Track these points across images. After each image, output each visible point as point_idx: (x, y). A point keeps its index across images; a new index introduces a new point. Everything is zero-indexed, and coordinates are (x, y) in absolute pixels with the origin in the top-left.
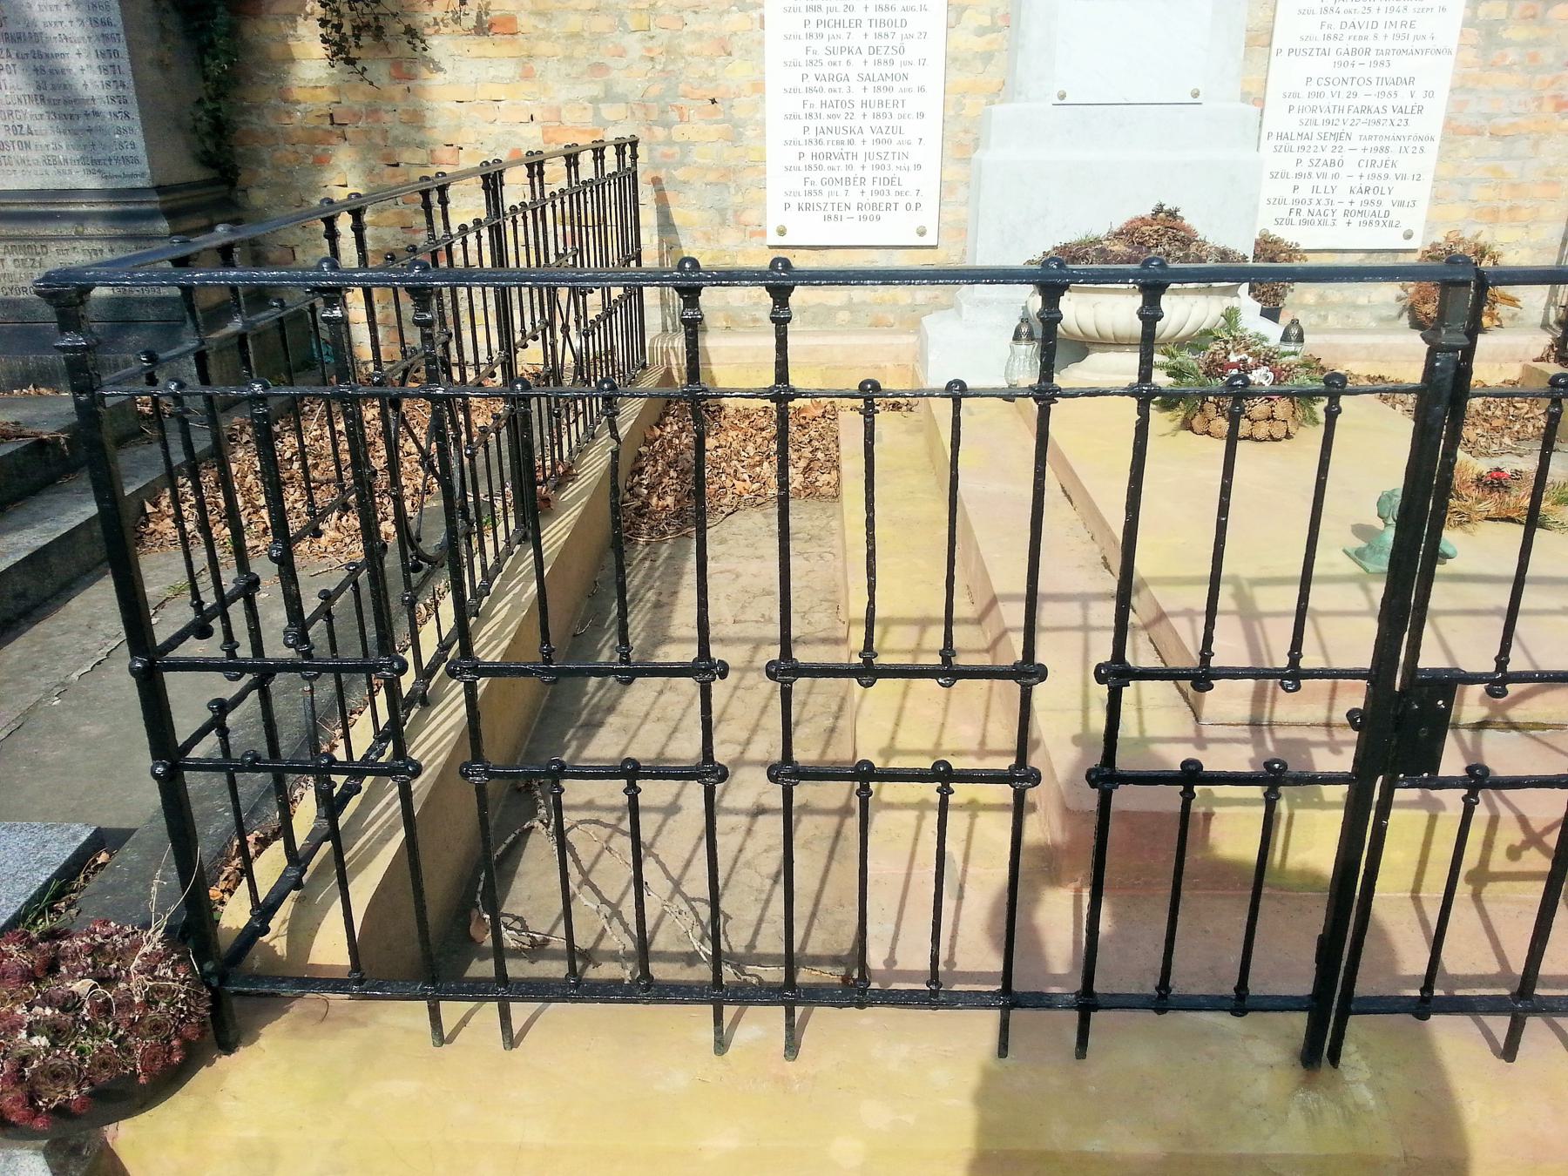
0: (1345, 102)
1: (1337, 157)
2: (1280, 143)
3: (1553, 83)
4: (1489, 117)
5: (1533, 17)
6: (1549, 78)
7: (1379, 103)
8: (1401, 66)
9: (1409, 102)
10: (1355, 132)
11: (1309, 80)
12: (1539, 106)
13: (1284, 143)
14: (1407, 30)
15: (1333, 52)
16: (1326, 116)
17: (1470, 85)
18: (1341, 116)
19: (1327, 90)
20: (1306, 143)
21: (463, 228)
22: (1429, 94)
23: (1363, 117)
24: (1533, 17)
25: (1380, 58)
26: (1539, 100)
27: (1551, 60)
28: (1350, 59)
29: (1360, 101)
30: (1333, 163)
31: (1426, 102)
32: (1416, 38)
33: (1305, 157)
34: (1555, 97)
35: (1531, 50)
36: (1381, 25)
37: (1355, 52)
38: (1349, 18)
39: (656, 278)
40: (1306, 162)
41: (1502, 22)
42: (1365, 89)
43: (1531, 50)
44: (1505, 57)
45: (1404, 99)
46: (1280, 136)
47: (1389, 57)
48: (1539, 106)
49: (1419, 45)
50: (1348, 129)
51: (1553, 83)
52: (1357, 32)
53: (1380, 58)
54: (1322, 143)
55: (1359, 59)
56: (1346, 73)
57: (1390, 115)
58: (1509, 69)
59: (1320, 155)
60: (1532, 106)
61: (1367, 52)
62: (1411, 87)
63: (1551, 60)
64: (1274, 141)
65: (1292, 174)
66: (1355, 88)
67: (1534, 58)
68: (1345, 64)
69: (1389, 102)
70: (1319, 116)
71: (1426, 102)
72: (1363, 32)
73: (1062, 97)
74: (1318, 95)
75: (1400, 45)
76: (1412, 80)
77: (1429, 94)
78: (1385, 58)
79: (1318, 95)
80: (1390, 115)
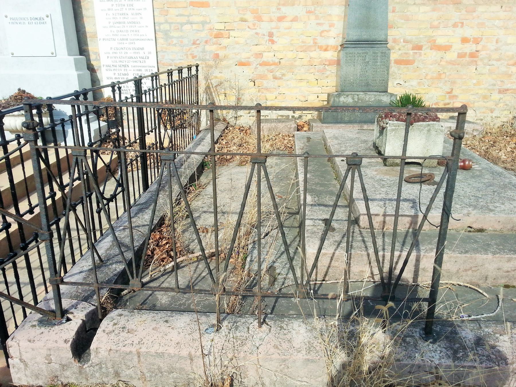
0: (125, 56)
1: (126, 72)
2: (107, 68)
3: (189, 50)
4: (173, 60)
5: (178, 29)
7: (136, 55)
8: (138, 44)
9: (144, 56)
10: (130, 64)
11: (111, 48)
12: (187, 57)
13: (109, 68)
14: (138, 33)
15: (116, 40)
16: (120, 60)
17: (164, 50)
18: (124, 60)
19: (118, 51)
20: (115, 68)
22: (150, 53)
23: (131, 60)
24: (178, 29)
25: (131, 42)
28: (122, 42)
29: (129, 55)
30: (125, 75)
31: (149, 55)
32: (141, 35)
33: (117, 72)
35: (180, 39)
36: (129, 31)
37: (123, 39)
38: (119, 29)
39: (204, 107)
40: (117, 74)
41: (169, 31)
42: (129, 51)
43: (180, 39)
44: (172, 41)
45: (142, 54)
46: (107, 66)
47: (134, 41)
48: (187, 57)
49: (142, 38)
50: (127, 64)
51: (189, 50)
52: (122, 33)
53: (131, 42)
54: (120, 68)
55: (125, 42)
56: (123, 46)
57: (139, 59)
58: (175, 45)
59: (120, 72)
60: (185, 57)
61: (127, 40)
62: (143, 51)
64: (105, 68)
65: (114, 78)
66: (126, 51)
67: (182, 42)
68: (121, 43)
69: (138, 55)
70: (118, 60)
71: (149, 55)
72: (124, 33)
73: (13, 54)
74: (116, 53)
75: (137, 37)
76: (143, 49)
77: (150, 53)
78: (133, 41)
79: (116, 53)
80: (139, 59)
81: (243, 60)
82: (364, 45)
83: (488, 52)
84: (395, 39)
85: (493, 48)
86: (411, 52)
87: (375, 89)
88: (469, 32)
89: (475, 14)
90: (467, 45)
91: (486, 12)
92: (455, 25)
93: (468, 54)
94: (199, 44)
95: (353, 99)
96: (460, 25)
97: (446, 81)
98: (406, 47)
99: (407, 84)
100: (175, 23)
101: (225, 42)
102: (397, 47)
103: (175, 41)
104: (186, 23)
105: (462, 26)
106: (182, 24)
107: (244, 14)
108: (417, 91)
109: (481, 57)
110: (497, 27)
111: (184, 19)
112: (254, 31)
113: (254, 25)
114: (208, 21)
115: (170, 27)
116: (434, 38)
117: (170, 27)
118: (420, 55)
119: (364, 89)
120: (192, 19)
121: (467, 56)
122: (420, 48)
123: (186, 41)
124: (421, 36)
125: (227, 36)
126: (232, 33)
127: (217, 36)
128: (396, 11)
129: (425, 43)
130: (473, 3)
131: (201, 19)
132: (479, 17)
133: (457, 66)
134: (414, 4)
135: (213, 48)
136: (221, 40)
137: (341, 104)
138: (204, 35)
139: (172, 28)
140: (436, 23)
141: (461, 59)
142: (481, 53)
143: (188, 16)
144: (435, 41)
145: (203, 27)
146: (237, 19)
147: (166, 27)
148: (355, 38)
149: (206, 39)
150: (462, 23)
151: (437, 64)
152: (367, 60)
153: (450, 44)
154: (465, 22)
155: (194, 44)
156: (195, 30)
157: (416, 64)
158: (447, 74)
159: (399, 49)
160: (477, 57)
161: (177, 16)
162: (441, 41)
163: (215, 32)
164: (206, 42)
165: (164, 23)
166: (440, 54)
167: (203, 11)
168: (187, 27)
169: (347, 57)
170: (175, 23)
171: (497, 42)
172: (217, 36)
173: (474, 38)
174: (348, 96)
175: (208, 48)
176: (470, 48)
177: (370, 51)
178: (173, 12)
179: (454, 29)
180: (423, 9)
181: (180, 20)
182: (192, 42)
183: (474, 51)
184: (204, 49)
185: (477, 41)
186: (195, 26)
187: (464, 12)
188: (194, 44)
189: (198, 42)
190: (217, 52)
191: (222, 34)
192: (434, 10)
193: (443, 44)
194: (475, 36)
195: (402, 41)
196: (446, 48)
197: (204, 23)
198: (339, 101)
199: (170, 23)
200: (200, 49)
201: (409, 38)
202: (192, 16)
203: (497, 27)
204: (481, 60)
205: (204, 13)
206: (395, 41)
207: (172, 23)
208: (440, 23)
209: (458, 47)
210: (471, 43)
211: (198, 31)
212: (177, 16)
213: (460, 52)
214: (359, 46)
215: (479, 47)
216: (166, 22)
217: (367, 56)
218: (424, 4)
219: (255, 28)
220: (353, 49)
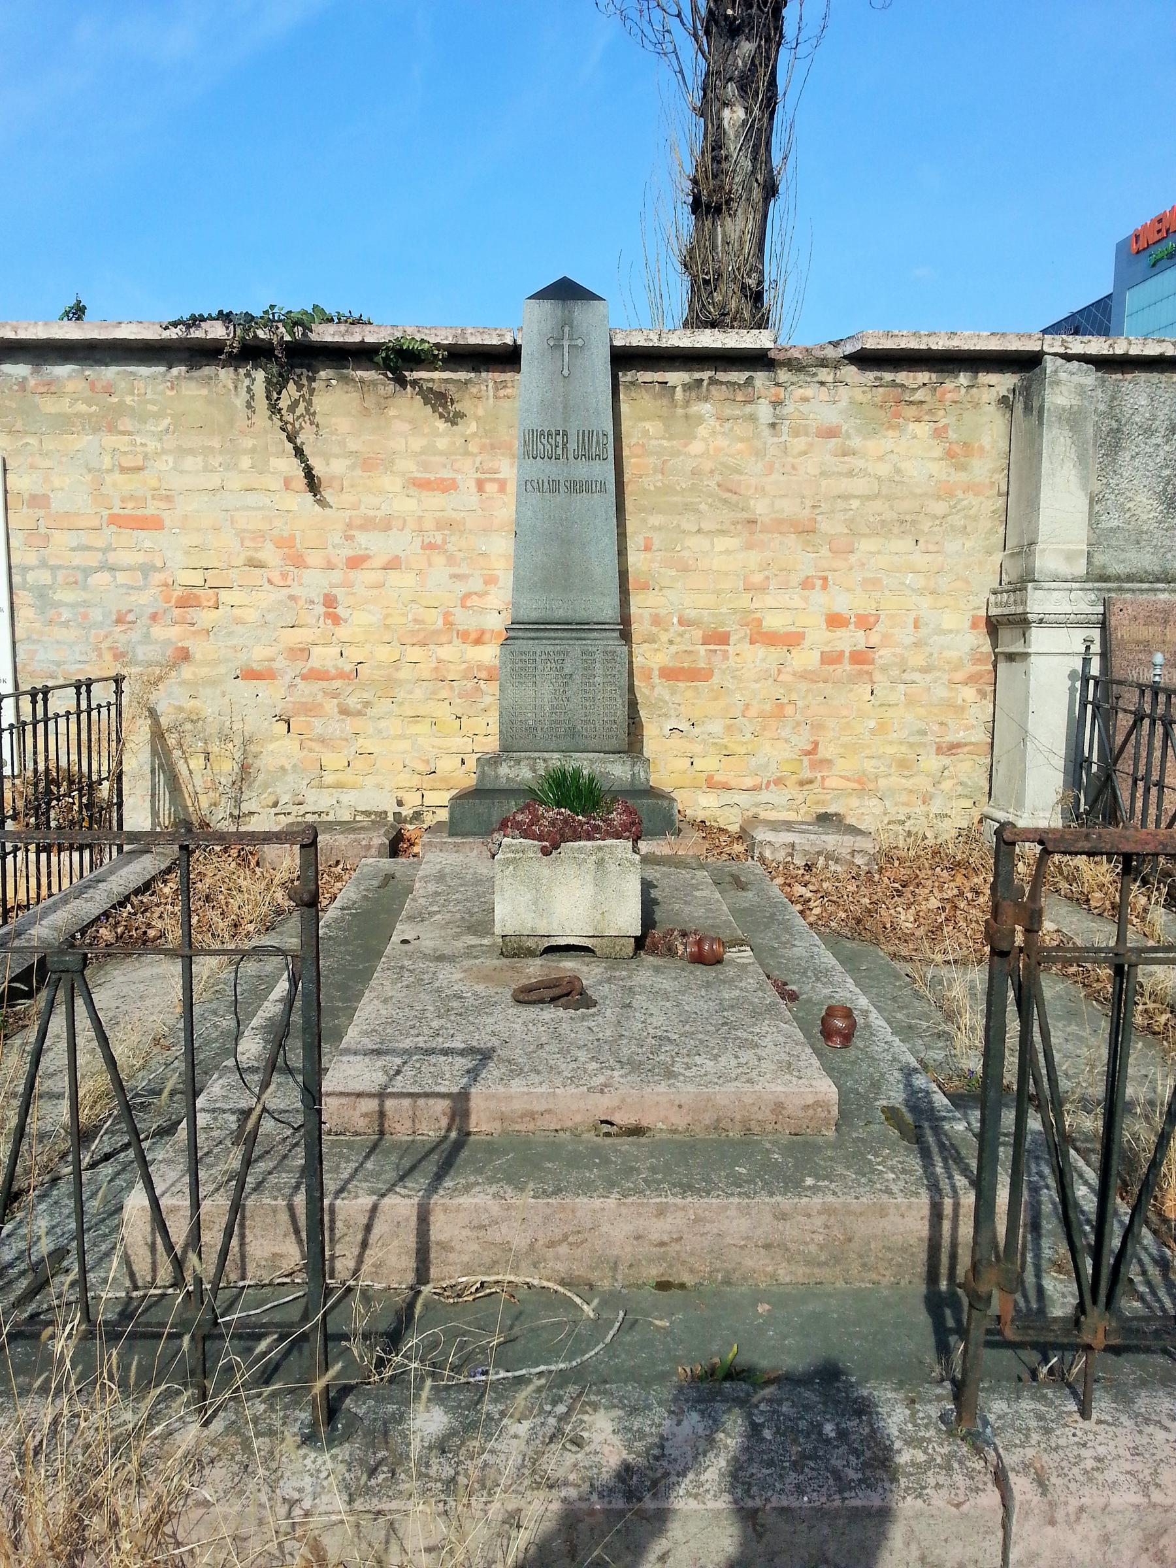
4: (58, 664)
5: (76, 583)
6: (102, 633)
12: (100, 656)
17: (35, 637)
21: (57, 716)
24: (76, 583)
26: (98, 650)
27: (100, 618)
34: (110, 648)
35: (82, 610)
43: (82, 610)
48: (100, 656)
58: (66, 624)
63: (100, 618)
67: (85, 616)
81: (255, 666)
82: (560, 634)
83: (898, 650)
84: (657, 615)
85: (908, 640)
86: (702, 649)
87: (593, 743)
88: (842, 603)
89: (853, 559)
90: (840, 632)
91: (879, 552)
92: (806, 584)
93: (847, 654)
94: (134, 622)
95: (535, 771)
96: (819, 583)
97: (798, 724)
98: (687, 636)
99: (697, 730)
100: (67, 568)
101: (205, 617)
102: (664, 637)
103: (66, 614)
104: (98, 570)
105: (824, 587)
106: (87, 572)
107: (257, 549)
108: (726, 747)
109: (879, 662)
110: (913, 590)
111: (93, 559)
112: (285, 591)
113: (284, 576)
114: (159, 564)
115: (54, 578)
117: (54, 578)
118: (726, 657)
119: (564, 743)
120: (112, 558)
121: (846, 661)
122: (724, 639)
123: (96, 615)
124: (724, 610)
125: (210, 604)
126: (224, 595)
127: (183, 604)
128: (654, 548)
129: (735, 627)
130: (846, 531)
131: (139, 558)
132: (863, 564)
133: (821, 685)
134: (698, 531)
135: (173, 633)
136: (192, 613)
137: (502, 783)
138: (146, 599)
139: (60, 579)
140: (757, 578)
142: (881, 652)
143: (104, 551)
144: (760, 621)
145: (145, 578)
146: (240, 561)
147: (45, 577)
148: (534, 616)
149: (154, 610)
150: (825, 579)
151: (771, 681)
152: (567, 671)
154: (830, 575)
155: (119, 621)
156: (122, 586)
157: (715, 680)
158: (800, 704)
159: (671, 642)
160: (872, 663)
161: (73, 550)
162: (774, 622)
163: (178, 592)
164: (154, 617)
165: (38, 567)
166: (776, 654)
167: (146, 538)
168: (103, 577)
169: (514, 662)
170: (67, 568)
171: (916, 627)
172: (183, 604)
173: (857, 616)
174: (518, 762)
175: (157, 632)
176: (849, 639)
177: (575, 649)
178: (62, 540)
179: (806, 592)
180: (722, 543)
181: (78, 559)
182: (114, 618)
183: (861, 646)
184: (147, 637)
185: (866, 623)
186: (122, 578)
187: (824, 551)
188: (119, 621)
189: (131, 617)
190: (186, 644)
191: (197, 597)
192: (749, 547)
193: (783, 630)
194: (861, 612)
195: (675, 620)
196: (791, 640)
197: (146, 570)
198: (497, 777)
199: (54, 569)
200: (135, 635)
201: (692, 614)
202: (115, 549)
203: (913, 590)
204: (884, 669)
205: (147, 544)
206: (656, 621)
207: (59, 567)
208: (767, 578)
209: (819, 637)
210: (852, 627)
211: (132, 588)
212: (73, 550)
213: (827, 649)
214: (546, 634)
215: (874, 639)
216: (43, 564)
217: (568, 660)
218: (722, 532)
219: (288, 583)
220: (531, 642)
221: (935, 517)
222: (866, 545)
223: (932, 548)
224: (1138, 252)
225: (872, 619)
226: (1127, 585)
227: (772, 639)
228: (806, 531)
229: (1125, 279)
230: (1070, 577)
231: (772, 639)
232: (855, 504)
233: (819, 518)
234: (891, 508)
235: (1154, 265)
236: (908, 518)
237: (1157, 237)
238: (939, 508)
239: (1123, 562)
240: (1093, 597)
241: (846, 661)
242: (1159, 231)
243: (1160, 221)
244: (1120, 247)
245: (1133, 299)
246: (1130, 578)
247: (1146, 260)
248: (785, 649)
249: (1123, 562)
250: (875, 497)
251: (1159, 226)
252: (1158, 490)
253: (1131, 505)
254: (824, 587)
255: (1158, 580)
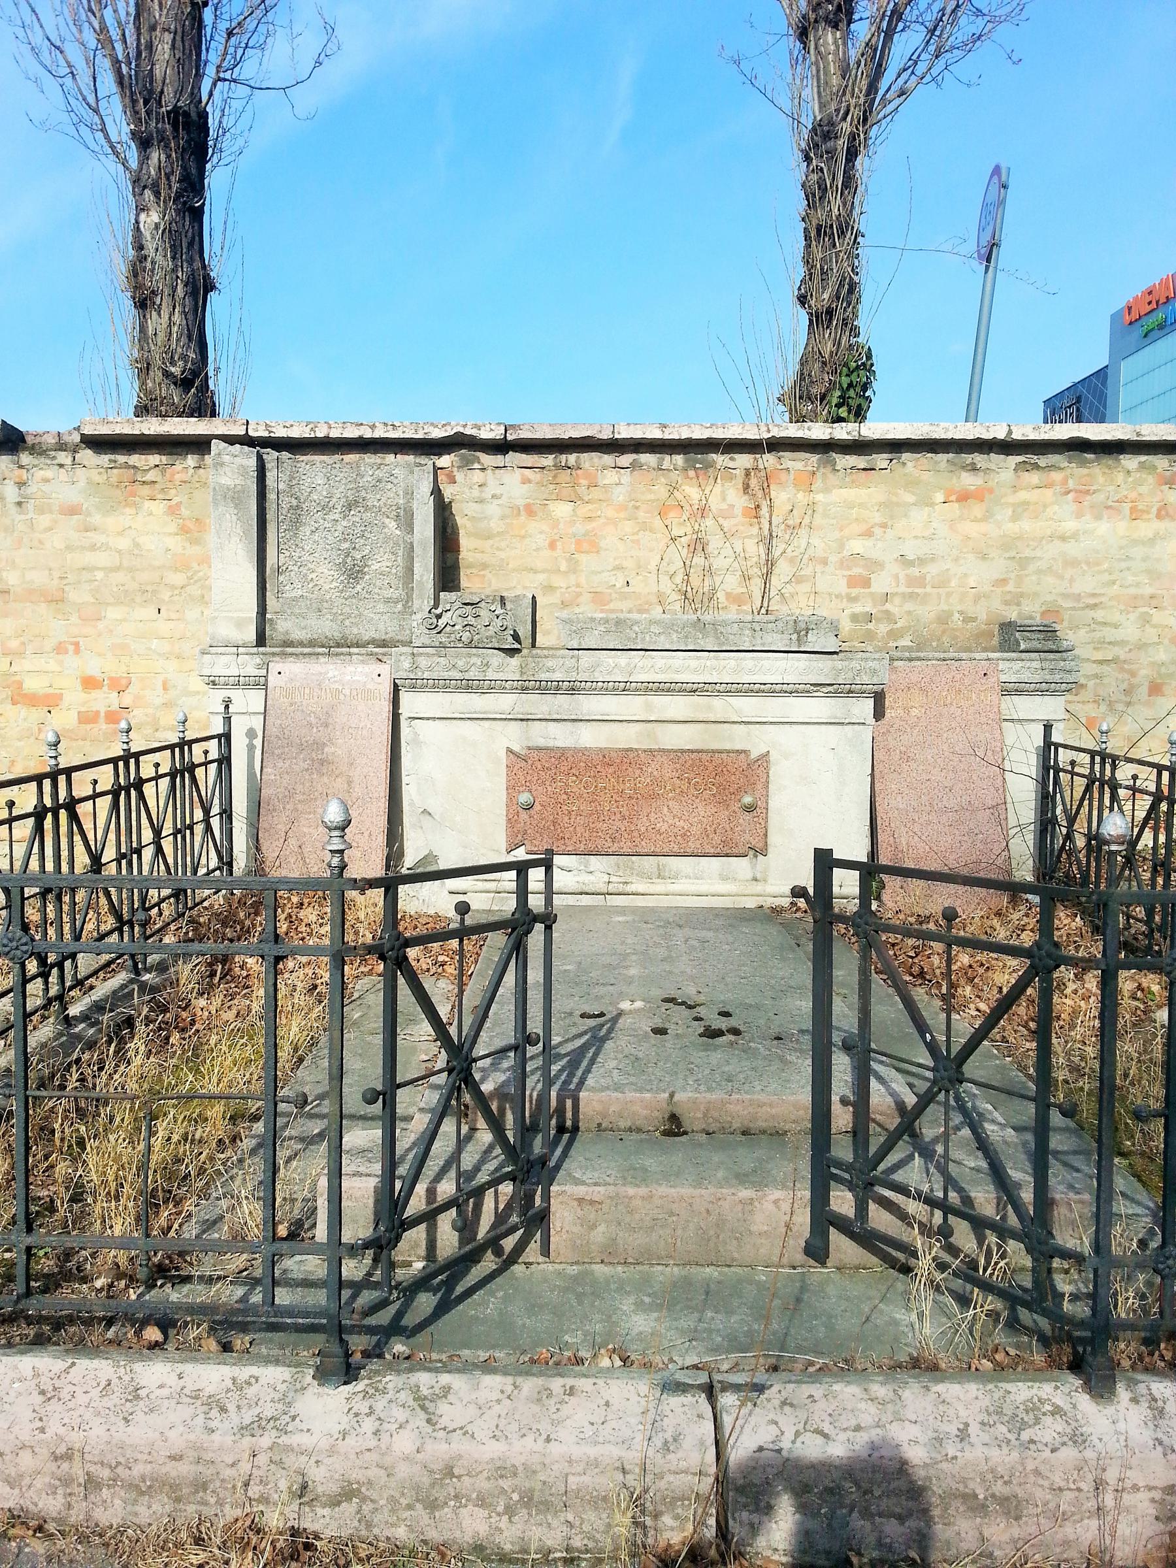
83: (150, 711)
85: (159, 701)
88: (94, 666)
89: (101, 625)
90: (95, 694)
91: (125, 620)
92: (60, 649)
93: (102, 714)
96: (71, 648)
105: (77, 651)
110: (159, 654)
116: (17, 678)
121: (102, 719)
130: (93, 600)
132: (111, 631)
133: (81, 743)
140: (14, 644)
141: (89, 727)
144: (20, 684)
150: (77, 644)
151: (32, 739)
153: (58, 691)
154: (81, 641)
162: (33, 684)
166: (37, 714)
171: (165, 689)
173: (111, 679)
176: (104, 700)
179: (60, 657)
183: (115, 707)
187: (74, 619)
193: (42, 692)
196: (50, 702)
203: (159, 654)
209: (75, 699)
210: (105, 688)
215: (127, 700)
221: (173, 587)
222: (113, 613)
223: (174, 616)
224: (1131, 323)
225: (124, 682)
226: (289, 650)
227: (32, 700)
228: (57, 600)
229: (1119, 352)
230: (240, 643)
231: (32, 700)
232: (99, 575)
233: (67, 588)
234: (133, 578)
235: (1145, 336)
236: (149, 588)
237: (1149, 308)
238: (178, 579)
239: (305, 628)
240: (258, 661)
241: (102, 719)
242: (1150, 303)
243: (1150, 293)
244: (1114, 317)
245: (1127, 369)
246: (312, 643)
247: (1138, 331)
248: (47, 709)
249: (305, 628)
250: (117, 569)
251: (1149, 298)
252: (337, 562)
253: (313, 575)
254: (77, 651)
255: (338, 645)
